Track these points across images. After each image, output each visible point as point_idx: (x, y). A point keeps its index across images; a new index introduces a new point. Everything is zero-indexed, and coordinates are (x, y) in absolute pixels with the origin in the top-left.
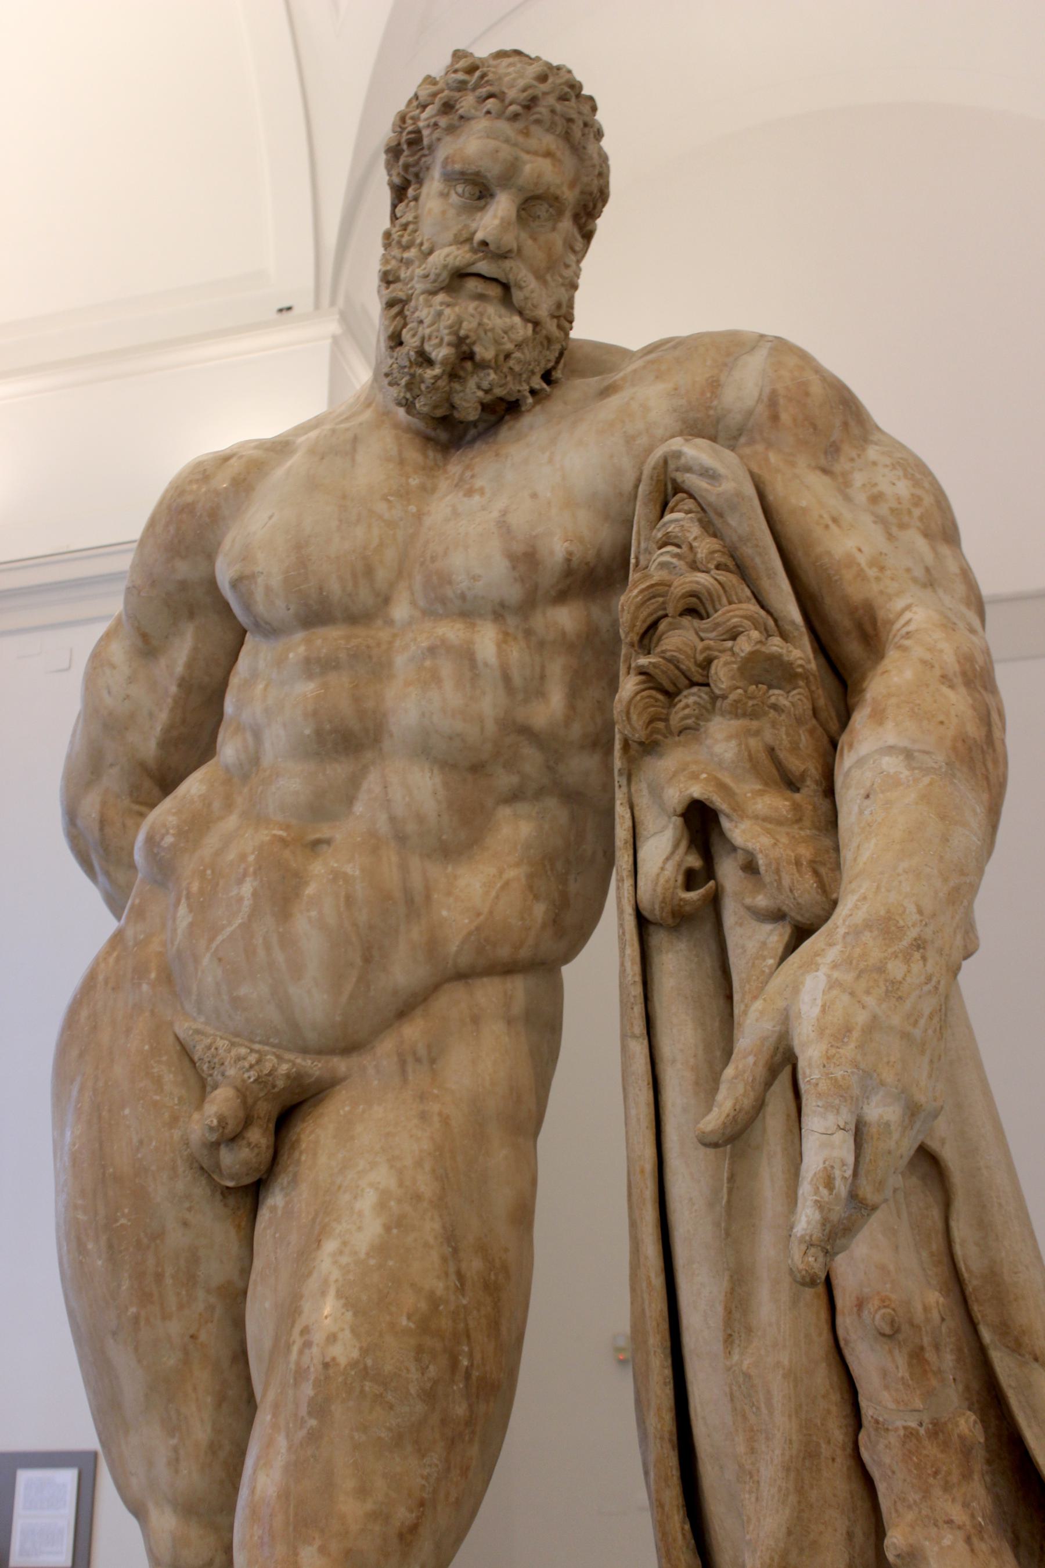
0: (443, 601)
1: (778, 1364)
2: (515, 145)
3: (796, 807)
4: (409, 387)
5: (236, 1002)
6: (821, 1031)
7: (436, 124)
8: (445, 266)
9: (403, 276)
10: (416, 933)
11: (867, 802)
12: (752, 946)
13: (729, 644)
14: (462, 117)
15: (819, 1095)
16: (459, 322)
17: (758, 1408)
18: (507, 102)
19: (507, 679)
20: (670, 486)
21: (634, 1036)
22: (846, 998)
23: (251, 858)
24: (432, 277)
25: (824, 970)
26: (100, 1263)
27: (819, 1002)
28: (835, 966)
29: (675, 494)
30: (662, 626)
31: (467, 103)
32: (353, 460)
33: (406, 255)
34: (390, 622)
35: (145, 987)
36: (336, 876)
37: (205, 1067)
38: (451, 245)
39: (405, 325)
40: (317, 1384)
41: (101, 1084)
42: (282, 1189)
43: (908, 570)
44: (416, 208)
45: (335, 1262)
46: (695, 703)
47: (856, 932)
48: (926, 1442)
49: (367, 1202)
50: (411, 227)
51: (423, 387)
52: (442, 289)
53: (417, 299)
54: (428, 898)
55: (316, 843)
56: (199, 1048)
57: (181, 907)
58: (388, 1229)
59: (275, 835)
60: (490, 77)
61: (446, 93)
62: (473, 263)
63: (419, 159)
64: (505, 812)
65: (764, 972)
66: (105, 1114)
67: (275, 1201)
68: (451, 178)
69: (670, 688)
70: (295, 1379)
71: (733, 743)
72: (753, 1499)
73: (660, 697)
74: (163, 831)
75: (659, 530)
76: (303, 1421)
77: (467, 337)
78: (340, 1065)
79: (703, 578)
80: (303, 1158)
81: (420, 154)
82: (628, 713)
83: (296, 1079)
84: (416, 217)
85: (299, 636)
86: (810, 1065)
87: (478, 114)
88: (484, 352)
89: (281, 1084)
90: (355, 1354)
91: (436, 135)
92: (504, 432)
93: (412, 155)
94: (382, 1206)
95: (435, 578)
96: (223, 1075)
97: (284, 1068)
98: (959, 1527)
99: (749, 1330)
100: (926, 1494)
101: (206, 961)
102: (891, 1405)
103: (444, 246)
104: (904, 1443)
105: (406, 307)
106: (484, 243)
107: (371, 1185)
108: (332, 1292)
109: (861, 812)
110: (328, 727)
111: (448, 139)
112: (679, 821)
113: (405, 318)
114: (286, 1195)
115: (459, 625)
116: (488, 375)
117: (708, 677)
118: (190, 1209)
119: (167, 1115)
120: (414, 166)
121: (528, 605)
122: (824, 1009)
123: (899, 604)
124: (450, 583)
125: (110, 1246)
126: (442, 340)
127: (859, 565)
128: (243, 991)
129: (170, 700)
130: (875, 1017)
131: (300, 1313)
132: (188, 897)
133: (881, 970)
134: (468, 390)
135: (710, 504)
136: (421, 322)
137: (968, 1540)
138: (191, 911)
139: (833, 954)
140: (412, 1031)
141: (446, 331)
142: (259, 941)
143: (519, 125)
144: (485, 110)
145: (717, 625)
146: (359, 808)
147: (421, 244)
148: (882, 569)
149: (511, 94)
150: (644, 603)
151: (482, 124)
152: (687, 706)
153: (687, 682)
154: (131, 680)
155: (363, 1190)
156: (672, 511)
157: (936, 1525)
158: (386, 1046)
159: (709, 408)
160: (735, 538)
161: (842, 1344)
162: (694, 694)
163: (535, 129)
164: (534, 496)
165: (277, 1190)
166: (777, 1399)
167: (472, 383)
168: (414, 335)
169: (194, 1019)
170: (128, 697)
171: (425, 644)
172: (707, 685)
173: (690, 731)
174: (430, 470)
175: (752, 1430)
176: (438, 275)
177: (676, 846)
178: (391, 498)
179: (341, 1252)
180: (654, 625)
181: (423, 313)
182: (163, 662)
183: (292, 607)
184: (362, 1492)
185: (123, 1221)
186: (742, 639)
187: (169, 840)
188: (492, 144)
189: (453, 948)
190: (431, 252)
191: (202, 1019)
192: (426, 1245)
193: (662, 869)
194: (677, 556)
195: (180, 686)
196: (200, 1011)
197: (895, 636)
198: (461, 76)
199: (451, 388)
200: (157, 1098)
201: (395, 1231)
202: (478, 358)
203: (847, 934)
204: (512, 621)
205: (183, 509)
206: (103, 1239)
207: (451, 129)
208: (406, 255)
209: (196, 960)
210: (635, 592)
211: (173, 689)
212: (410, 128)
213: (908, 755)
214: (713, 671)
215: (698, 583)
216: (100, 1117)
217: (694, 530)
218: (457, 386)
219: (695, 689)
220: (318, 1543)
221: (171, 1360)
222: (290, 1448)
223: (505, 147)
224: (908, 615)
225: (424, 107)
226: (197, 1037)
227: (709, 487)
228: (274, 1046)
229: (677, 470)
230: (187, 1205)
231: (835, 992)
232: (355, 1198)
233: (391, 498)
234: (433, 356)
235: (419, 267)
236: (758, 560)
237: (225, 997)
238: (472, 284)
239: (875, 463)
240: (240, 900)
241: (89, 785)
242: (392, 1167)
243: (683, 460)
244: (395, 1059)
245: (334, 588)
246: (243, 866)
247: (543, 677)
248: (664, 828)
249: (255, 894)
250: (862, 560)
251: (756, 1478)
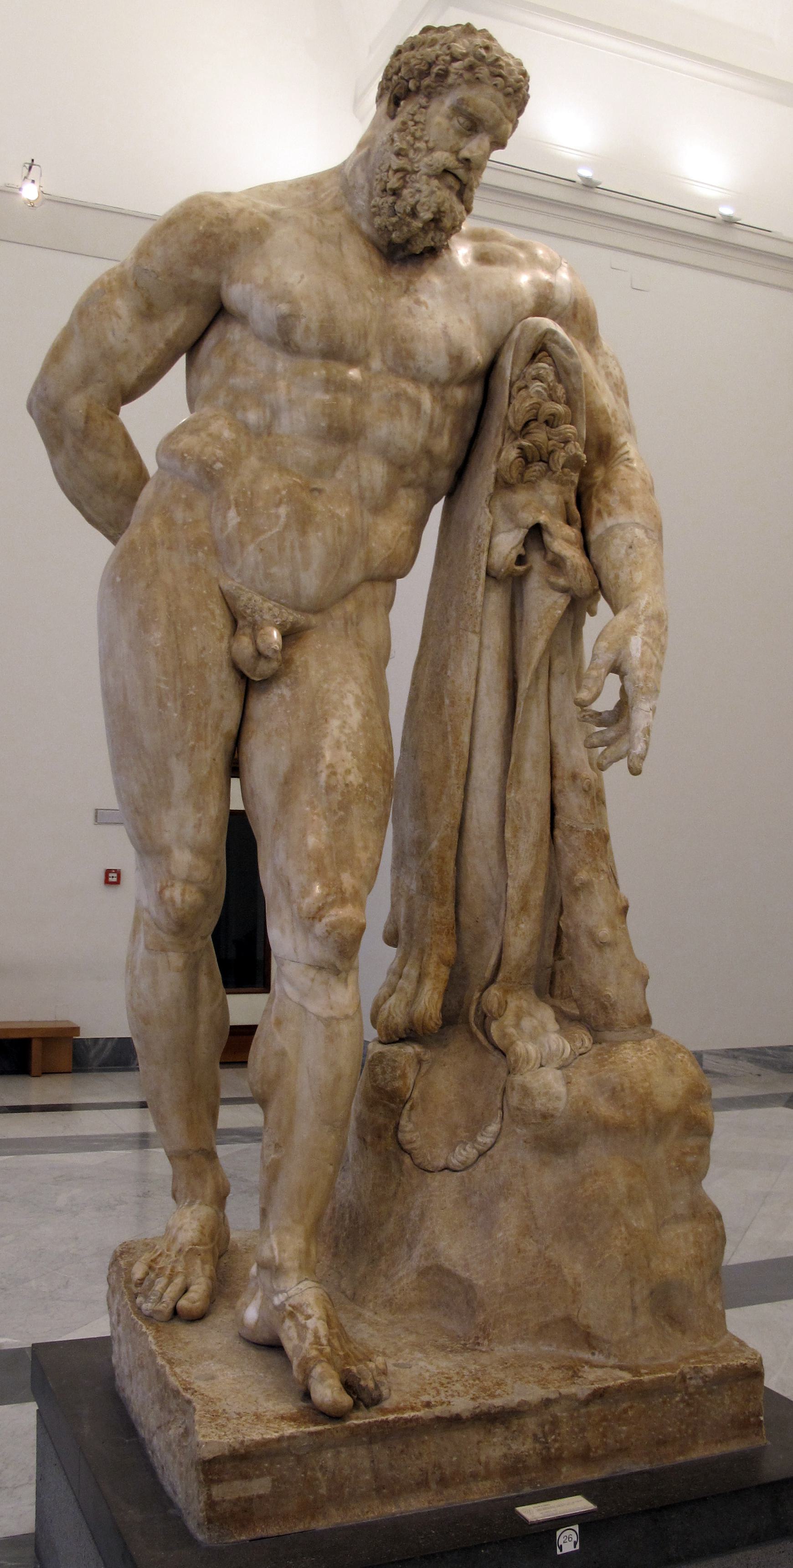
0: (406, 368)
1: (535, 799)
2: (503, 111)
3: (576, 537)
4: (394, 225)
5: (268, 576)
6: (642, 664)
7: (461, 75)
8: (444, 165)
9: (411, 154)
10: (362, 554)
11: (630, 551)
12: (549, 601)
13: (563, 445)
14: (478, 78)
15: (643, 694)
16: (444, 202)
17: (521, 818)
18: (508, 84)
19: (431, 423)
20: (540, 346)
21: (474, 632)
22: (649, 650)
23: (284, 492)
24: (434, 167)
25: (640, 635)
26: (176, 715)
27: (640, 651)
28: (644, 635)
29: (540, 351)
30: (533, 425)
31: (484, 72)
32: (341, 250)
33: (418, 145)
34: (368, 368)
35: (200, 554)
36: (333, 516)
37: (248, 611)
38: (446, 151)
39: (404, 187)
40: (343, 794)
41: (173, 608)
42: (287, 686)
43: (624, 422)
44: (426, 113)
45: (341, 732)
46: (539, 470)
47: (648, 619)
48: (595, 837)
49: (350, 701)
50: (421, 126)
51: (405, 229)
52: (433, 176)
53: (420, 176)
54: (368, 535)
55: (313, 490)
56: (244, 598)
57: (231, 511)
58: (364, 716)
59: (295, 481)
60: (501, 63)
61: (472, 58)
62: (456, 168)
63: (438, 86)
64: (402, 493)
65: (555, 616)
66: (179, 628)
67: (281, 692)
68: (457, 110)
69: (530, 459)
70: (327, 791)
71: (554, 497)
72: (514, 857)
73: (524, 463)
74: (215, 459)
75: (534, 369)
76: (335, 813)
77: (444, 212)
78: (314, 620)
79: (560, 408)
80: (300, 670)
81: (439, 83)
82: (510, 467)
83: (293, 624)
84: (425, 121)
85: (317, 362)
86: (638, 680)
87: (489, 82)
88: (447, 222)
89: (288, 626)
90: (361, 781)
91: (459, 81)
92: (426, 265)
93: (435, 82)
94: (358, 704)
95: (404, 353)
96: (261, 617)
97: (291, 618)
98: (606, 873)
99: (519, 782)
100: (595, 859)
101: (251, 548)
102: (582, 821)
103: (442, 150)
104: (586, 837)
105: (408, 176)
106: (467, 160)
107: (350, 692)
108: (344, 747)
109: (628, 554)
110: (336, 425)
111: (464, 86)
112: (527, 531)
113: (405, 182)
114: (291, 690)
115: (412, 385)
116: (442, 236)
117: (549, 458)
118: (225, 690)
119: (218, 634)
120: (432, 88)
121: (446, 384)
122: (643, 654)
123: (622, 440)
124: (413, 359)
125: (183, 706)
126: (430, 207)
127: (608, 414)
128: (274, 570)
129: (156, 351)
130: (658, 661)
131: (323, 756)
132: (237, 505)
133: (659, 640)
134: (427, 239)
135: (564, 366)
137: (608, 878)
138: (239, 514)
139: (641, 628)
140: (350, 606)
141: (435, 205)
142: (287, 544)
143: (508, 99)
144: (494, 83)
145: (560, 434)
146: (339, 475)
147: (427, 142)
148: (616, 419)
149: (511, 80)
150: (528, 411)
151: (490, 91)
152: (535, 471)
153: (539, 459)
154: (131, 330)
155: (345, 694)
156: (540, 361)
157: (598, 871)
158: (338, 612)
159: (548, 299)
160: (570, 388)
161: (556, 792)
162: (540, 466)
163: (513, 105)
164: (461, 321)
165: (283, 686)
166: (533, 814)
167: (431, 234)
168: (411, 197)
169: (233, 579)
170: (126, 341)
171: (394, 391)
172: (547, 462)
173: (532, 484)
174: (385, 272)
175: (516, 827)
176: (438, 168)
177: (519, 543)
178: (373, 290)
179: (344, 727)
180: (527, 424)
181: (424, 188)
182: (157, 326)
183: (320, 345)
184: (366, 848)
185: (191, 692)
186: (570, 446)
187: (219, 466)
188: (494, 106)
189: (376, 565)
190: (431, 150)
191: (239, 580)
192: (379, 728)
193: (510, 552)
194: (545, 389)
195: (166, 345)
196: (239, 576)
197: (619, 458)
198: (483, 52)
199: (418, 234)
200: (214, 624)
201: (367, 718)
202: (442, 225)
203: (645, 620)
204: (437, 389)
205: (210, 236)
206: (179, 703)
207: (468, 82)
208: (418, 145)
209: (243, 545)
210: (527, 404)
211: (162, 345)
212: (441, 67)
213: (646, 532)
214: (556, 458)
215: (558, 410)
216: (175, 629)
217: (551, 378)
218: (421, 234)
219: (541, 463)
220: (349, 871)
221: (205, 772)
222: (329, 826)
223: (498, 110)
224: (626, 449)
225: (454, 59)
226: (240, 592)
227: (567, 358)
228: (282, 604)
229: (550, 340)
230: (225, 687)
231: (645, 647)
232: (342, 697)
233: (373, 290)
234: (422, 214)
235: (425, 156)
236: (579, 404)
237: (261, 572)
238: (450, 180)
239: (607, 354)
240: (278, 517)
241: (77, 389)
242: (356, 683)
243: (556, 337)
244: (343, 622)
245: (349, 339)
246: (278, 496)
247: (444, 425)
248: (510, 531)
249: (288, 516)
250: (610, 411)
251: (516, 848)
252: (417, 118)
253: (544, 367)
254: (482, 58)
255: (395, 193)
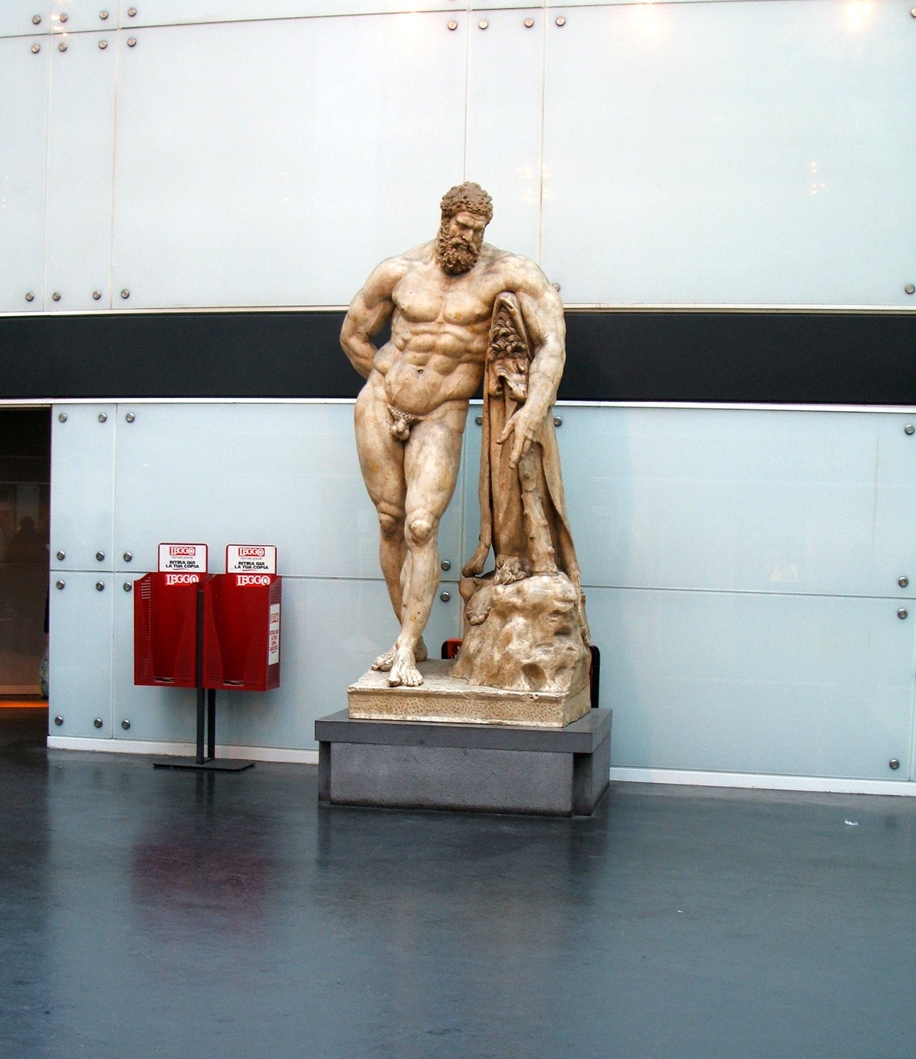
9: (445, 240)
31: (464, 207)
60: (470, 203)
97: (413, 418)
136: (449, 254)
151: (468, 213)
181: (450, 252)
190: (452, 237)
225: (454, 205)
252: (446, 227)
253: (503, 314)
254: (462, 202)
255: (442, 254)
